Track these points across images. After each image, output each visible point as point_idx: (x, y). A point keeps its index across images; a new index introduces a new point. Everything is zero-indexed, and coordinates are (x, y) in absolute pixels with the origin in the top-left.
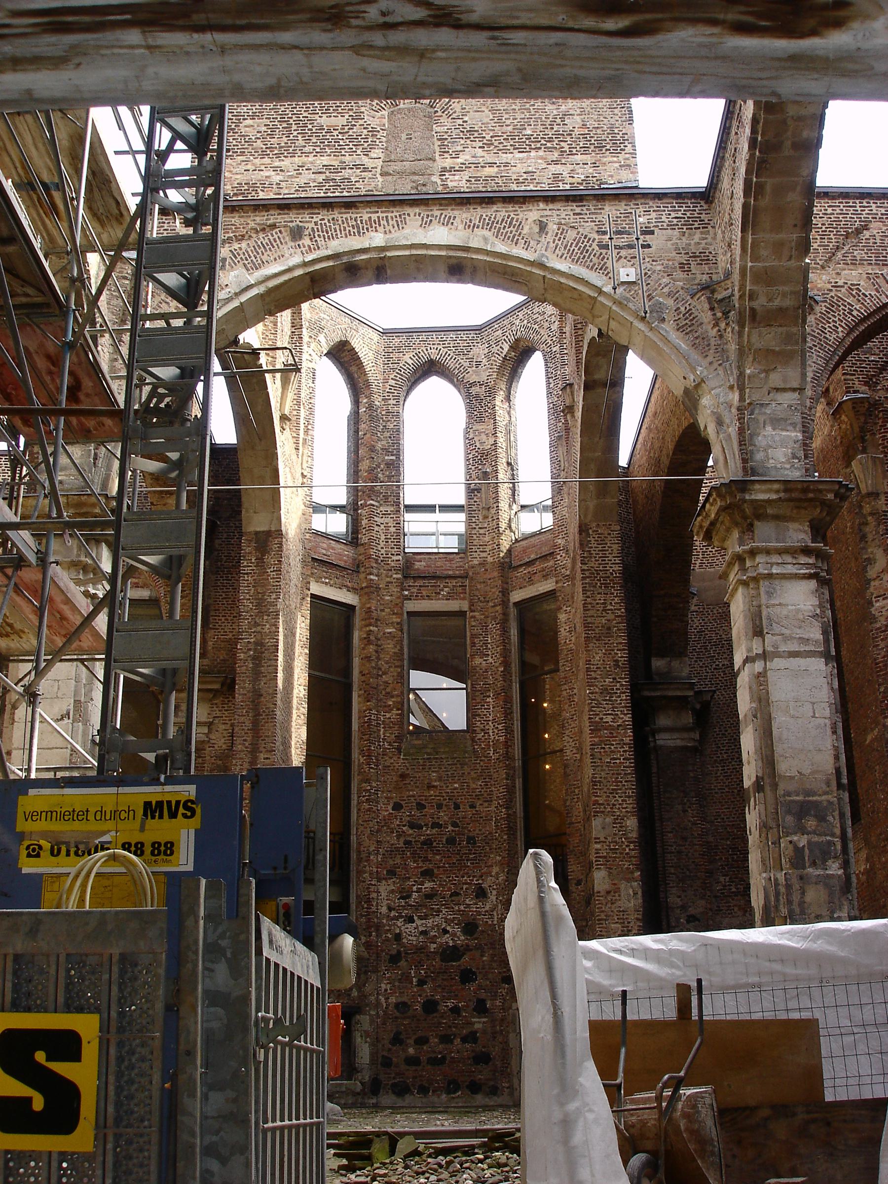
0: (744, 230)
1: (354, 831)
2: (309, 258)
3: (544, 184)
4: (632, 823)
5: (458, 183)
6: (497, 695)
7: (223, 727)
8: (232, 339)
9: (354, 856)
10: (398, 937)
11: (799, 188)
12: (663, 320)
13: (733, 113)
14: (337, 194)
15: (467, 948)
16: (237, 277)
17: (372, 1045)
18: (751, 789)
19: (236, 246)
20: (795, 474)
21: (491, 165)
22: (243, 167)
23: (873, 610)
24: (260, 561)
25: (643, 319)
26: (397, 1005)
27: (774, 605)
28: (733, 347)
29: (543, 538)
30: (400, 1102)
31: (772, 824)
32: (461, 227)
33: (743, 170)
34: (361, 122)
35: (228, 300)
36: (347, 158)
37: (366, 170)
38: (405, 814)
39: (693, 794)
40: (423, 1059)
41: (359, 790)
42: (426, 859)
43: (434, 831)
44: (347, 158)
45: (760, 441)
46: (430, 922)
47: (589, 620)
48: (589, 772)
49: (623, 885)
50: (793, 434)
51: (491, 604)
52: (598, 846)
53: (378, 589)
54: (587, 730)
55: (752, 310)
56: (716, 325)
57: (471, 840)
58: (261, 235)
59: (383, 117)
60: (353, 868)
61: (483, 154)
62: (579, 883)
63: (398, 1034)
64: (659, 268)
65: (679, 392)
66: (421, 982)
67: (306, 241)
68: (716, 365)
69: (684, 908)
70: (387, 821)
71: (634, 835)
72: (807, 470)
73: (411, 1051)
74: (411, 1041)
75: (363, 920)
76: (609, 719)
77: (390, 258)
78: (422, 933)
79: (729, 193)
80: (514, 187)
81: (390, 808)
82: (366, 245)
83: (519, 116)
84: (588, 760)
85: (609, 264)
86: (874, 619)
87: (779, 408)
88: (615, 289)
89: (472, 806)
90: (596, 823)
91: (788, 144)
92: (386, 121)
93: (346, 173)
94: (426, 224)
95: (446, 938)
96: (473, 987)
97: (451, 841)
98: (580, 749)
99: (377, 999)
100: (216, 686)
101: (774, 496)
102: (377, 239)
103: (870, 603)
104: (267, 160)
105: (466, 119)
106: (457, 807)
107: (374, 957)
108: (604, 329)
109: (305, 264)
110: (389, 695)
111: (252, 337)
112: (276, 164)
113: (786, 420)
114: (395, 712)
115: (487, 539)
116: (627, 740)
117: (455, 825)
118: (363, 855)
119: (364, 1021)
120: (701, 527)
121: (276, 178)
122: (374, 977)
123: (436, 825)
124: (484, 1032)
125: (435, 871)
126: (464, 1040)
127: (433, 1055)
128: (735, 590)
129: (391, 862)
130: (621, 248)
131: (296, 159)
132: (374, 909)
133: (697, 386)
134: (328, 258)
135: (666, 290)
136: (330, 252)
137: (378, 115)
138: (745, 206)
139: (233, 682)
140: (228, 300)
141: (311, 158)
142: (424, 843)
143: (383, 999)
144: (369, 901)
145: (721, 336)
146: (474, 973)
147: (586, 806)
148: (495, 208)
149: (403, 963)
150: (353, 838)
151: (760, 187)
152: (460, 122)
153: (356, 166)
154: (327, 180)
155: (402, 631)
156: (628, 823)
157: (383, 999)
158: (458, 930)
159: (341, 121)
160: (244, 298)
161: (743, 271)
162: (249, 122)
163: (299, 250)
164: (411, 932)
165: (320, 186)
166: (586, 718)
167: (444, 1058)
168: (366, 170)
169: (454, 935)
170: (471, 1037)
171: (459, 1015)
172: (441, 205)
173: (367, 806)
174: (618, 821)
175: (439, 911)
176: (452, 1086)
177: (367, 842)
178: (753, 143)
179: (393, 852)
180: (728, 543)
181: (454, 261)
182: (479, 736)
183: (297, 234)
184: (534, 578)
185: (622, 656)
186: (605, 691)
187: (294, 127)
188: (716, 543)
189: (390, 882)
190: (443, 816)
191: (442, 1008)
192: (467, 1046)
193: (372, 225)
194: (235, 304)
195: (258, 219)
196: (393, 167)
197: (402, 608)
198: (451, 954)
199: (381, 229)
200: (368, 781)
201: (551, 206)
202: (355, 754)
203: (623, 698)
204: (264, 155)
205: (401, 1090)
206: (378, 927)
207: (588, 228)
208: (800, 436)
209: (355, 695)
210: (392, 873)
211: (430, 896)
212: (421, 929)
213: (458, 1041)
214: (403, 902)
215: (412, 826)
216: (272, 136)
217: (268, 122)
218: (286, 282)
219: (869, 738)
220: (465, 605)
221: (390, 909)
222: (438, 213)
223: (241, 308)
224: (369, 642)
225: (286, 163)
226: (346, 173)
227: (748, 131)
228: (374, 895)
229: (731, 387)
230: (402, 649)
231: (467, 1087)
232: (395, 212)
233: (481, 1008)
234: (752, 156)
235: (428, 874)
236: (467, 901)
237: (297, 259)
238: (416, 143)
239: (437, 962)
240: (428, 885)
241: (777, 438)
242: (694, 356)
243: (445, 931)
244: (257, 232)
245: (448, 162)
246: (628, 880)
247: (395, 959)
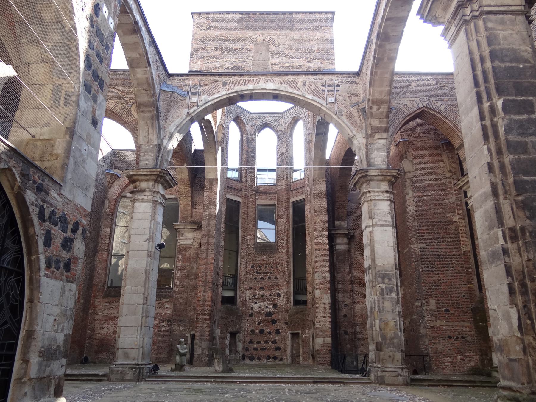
0: (370, 87)
1: (238, 274)
2: (228, 92)
3: (305, 70)
4: (328, 275)
5: (277, 68)
6: (285, 231)
7: (197, 240)
8: (203, 118)
9: (238, 282)
10: (252, 309)
11: (389, 73)
12: (342, 115)
13: (368, 47)
14: (237, 71)
15: (274, 313)
16: (205, 98)
17: (243, 343)
18: (367, 269)
19: (205, 88)
20: (384, 166)
21: (288, 62)
22: (207, 61)
23: (408, 210)
24: (211, 188)
25: (336, 115)
26: (251, 331)
27: (376, 209)
28: (364, 125)
29: (301, 181)
30: (251, 363)
31: (374, 281)
32: (277, 83)
33: (370, 67)
34: (245, 47)
35: (202, 106)
36: (241, 59)
37: (247, 63)
38: (255, 269)
39: (347, 265)
40: (259, 348)
41: (241, 261)
42: (261, 284)
43: (264, 275)
44: (241, 59)
45: (373, 155)
46: (262, 304)
47: (315, 209)
48: (314, 258)
49: (325, 295)
50: (384, 154)
51: (284, 202)
52: (317, 282)
53: (248, 196)
54: (314, 244)
55: (372, 113)
56: (359, 117)
57: (276, 278)
58: (213, 84)
59: (253, 46)
60: (238, 286)
61: (286, 59)
62: (310, 293)
63: (251, 340)
64: (342, 98)
65: (347, 138)
66: (259, 323)
67: (227, 87)
68: (359, 130)
69: (343, 301)
70: (249, 271)
71: (329, 279)
72: (388, 165)
73: (255, 346)
74: (255, 342)
75: (241, 303)
76: (321, 241)
77: (254, 93)
78: (260, 307)
79: (365, 74)
80: (295, 70)
81: (250, 267)
82: (247, 89)
83: (297, 46)
84: (314, 254)
85: (325, 97)
86: (408, 213)
87: (379, 145)
88: (327, 104)
89: (277, 267)
90: (316, 275)
91: (386, 58)
92: (253, 47)
93: (240, 64)
94: (266, 82)
95: (267, 310)
96: (275, 325)
97: (270, 278)
98: (312, 250)
99: (245, 329)
100: (196, 227)
101: (377, 174)
102: (250, 87)
103: (407, 208)
104: (214, 59)
105: (280, 47)
106: (272, 267)
107: (244, 315)
108: (323, 118)
109: (227, 94)
110: (251, 231)
111: (209, 117)
112: (218, 61)
113: (381, 149)
114: (253, 236)
115: (283, 181)
116: (327, 248)
117: (271, 273)
118: (242, 282)
119: (240, 336)
120: (353, 183)
121: (218, 65)
122: (244, 321)
123: (265, 273)
124: (279, 340)
125: (264, 287)
126: (272, 342)
127: (262, 347)
128: (363, 203)
129: (250, 284)
130: (329, 91)
131: (224, 59)
132: (244, 299)
133: (353, 137)
134: (234, 92)
135: (344, 105)
136: (235, 91)
137: (251, 45)
138: (371, 79)
139: (201, 226)
140: (202, 106)
141: (229, 59)
142: (261, 278)
143: (246, 329)
144: (243, 297)
145: (361, 121)
146: (276, 321)
147: (313, 269)
148: (289, 77)
149: (253, 317)
150: (238, 276)
151: (376, 72)
152: (278, 48)
153: (244, 62)
154: (234, 67)
155: (255, 210)
156: (327, 275)
157: (246, 329)
158: (271, 307)
159: (239, 47)
160: (207, 105)
161: (369, 100)
162: (209, 46)
163: (225, 90)
164: (256, 308)
165: (232, 68)
166: (314, 240)
167: (266, 348)
168: (247, 63)
169: (270, 308)
170: (275, 342)
171: (271, 334)
172: (271, 76)
173: (243, 266)
174: (323, 274)
175: (265, 300)
176: (268, 358)
177: (243, 278)
178: (374, 58)
179: (251, 281)
180: (361, 188)
181: (275, 94)
182: (279, 244)
183: (225, 84)
184: (298, 194)
185: (326, 221)
186: (320, 232)
187: (224, 48)
188: (357, 188)
189: (250, 291)
190: (267, 270)
191: (265, 332)
192: (273, 344)
193: (249, 82)
194: (204, 107)
195: (212, 79)
197: (255, 203)
198: (269, 314)
199: (251, 83)
200: (243, 258)
201: (307, 77)
202: (240, 250)
203: (326, 235)
204: (213, 58)
205: (252, 358)
206: (246, 305)
207: (319, 84)
208: (386, 154)
209: (240, 230)
210: (250, 288)
211: (262, 296)
212: (259, 306)
213: (270, 343)
214: (254, 297)
215: (257, 273)
216: (216, 51)
217: (215, 46)
218: (221, 100)
219: (405, 251)
220: (276, 202)
221: (250, 299)
222: (270, 78)
223: (206, 108)
224: (245, 214)
225: (221, 60)
226: (240, 64)
227: (373, 53)
228: (245, 295)
229: (364, 138)
230: (255, 216)
231: (273, 358)
232: (256, 78)
233: (278, 332)
234: (374, 62)
235: (262, 288)
236: (274, 298)
237: (224, 93)
238: (263, 55)
239: (264, 317)
240: (262, 292)
241: (378, 155)
242: (352, 128)
243: (267, 307)
244: (211, 83)
245: (274, 61)
246: (326, 293)
247: (251, 316)
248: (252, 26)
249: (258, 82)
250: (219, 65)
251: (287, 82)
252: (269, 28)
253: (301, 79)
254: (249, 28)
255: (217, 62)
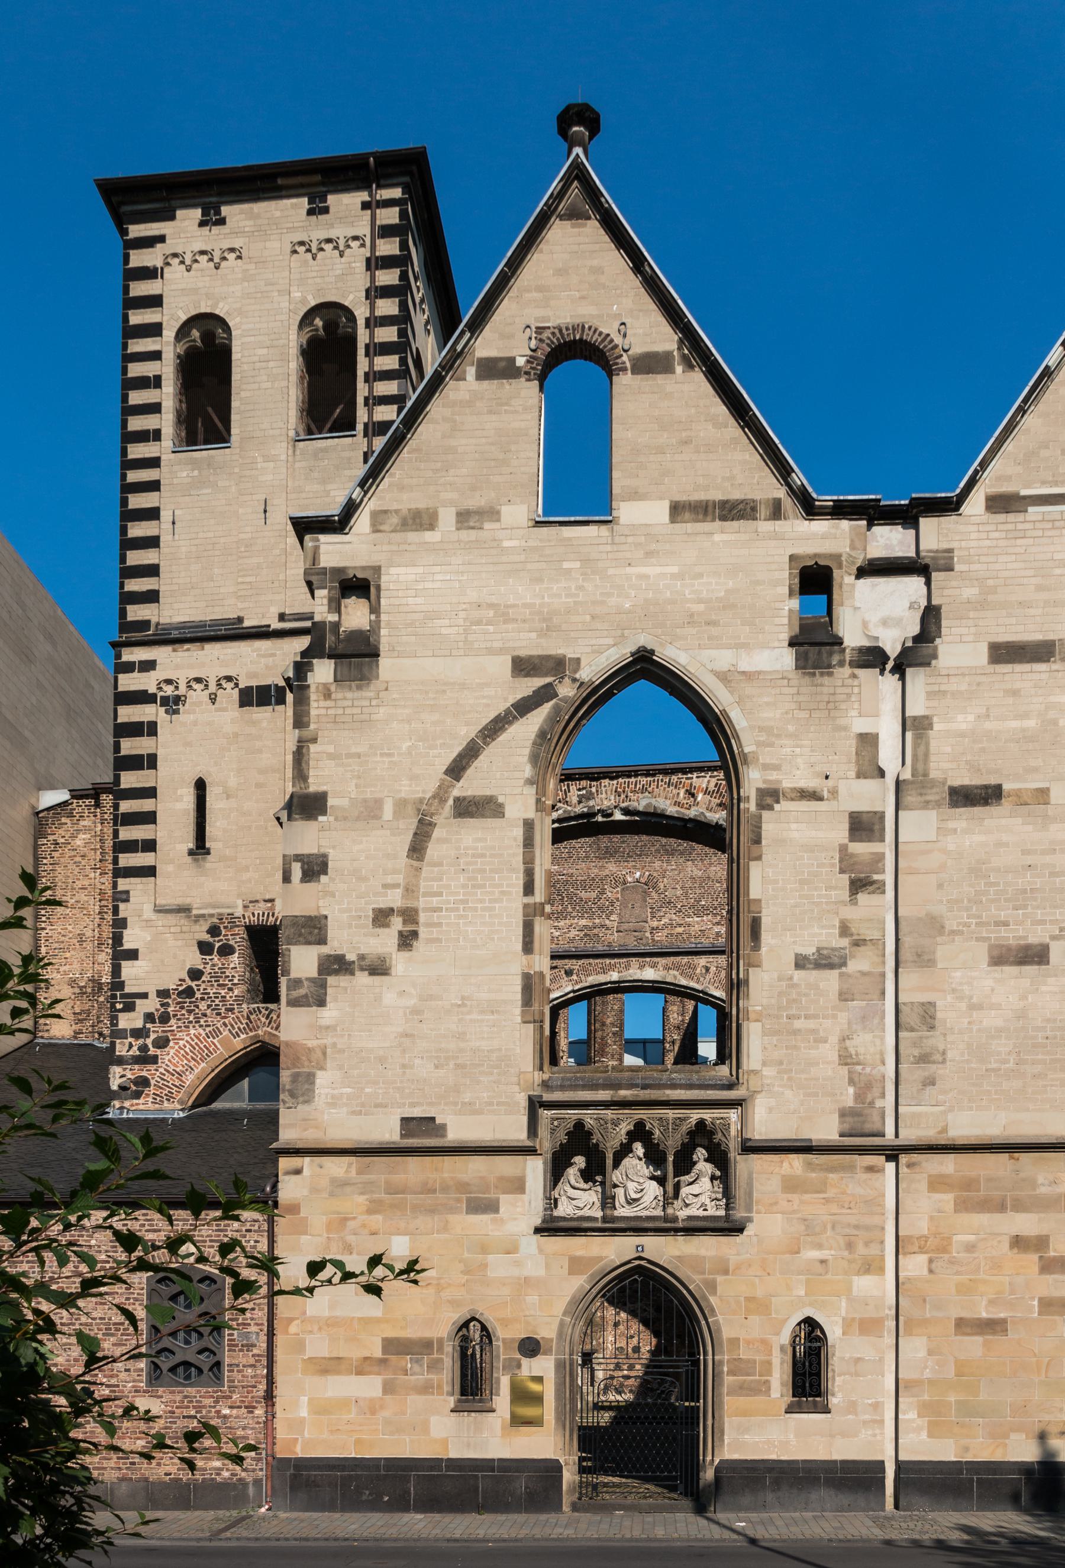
21: (680, 925)
83: (698, 891)
94: (642, 967)
102: (614, 976)
109: (574, 991)
141: (576, 921)
154: (586, 935)
159: (593, 895)
165: (581, 939)
196: (625, 926)
225: (562, 923)
238: (637, 911)
245: (655, 924)
248: (616, 852)
249: (628, 967)
250: (558, 934)
251: (677, 967)
252: (647, 855)
253: (702, 961)
254: (611, 855)
255: (555, 927)
